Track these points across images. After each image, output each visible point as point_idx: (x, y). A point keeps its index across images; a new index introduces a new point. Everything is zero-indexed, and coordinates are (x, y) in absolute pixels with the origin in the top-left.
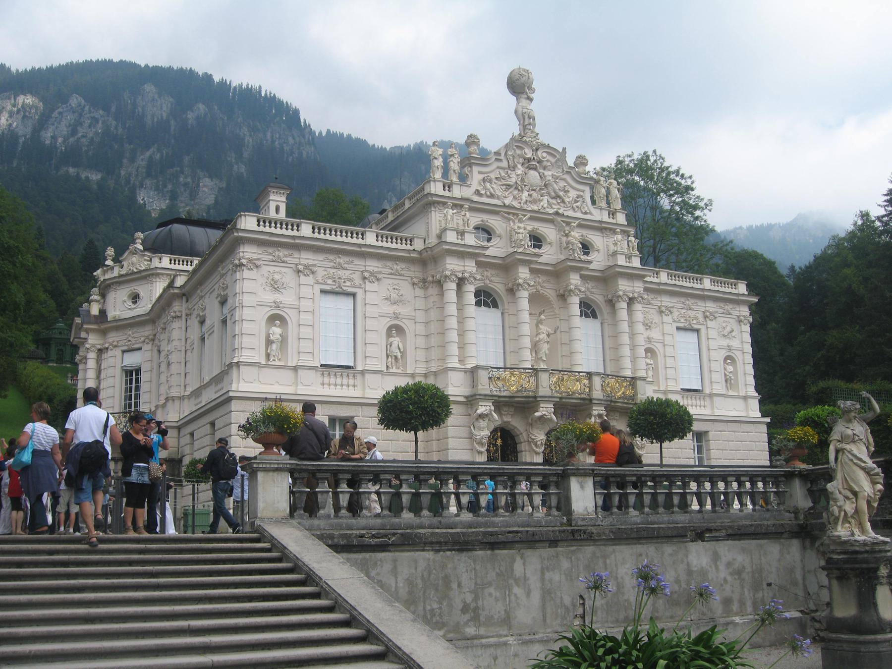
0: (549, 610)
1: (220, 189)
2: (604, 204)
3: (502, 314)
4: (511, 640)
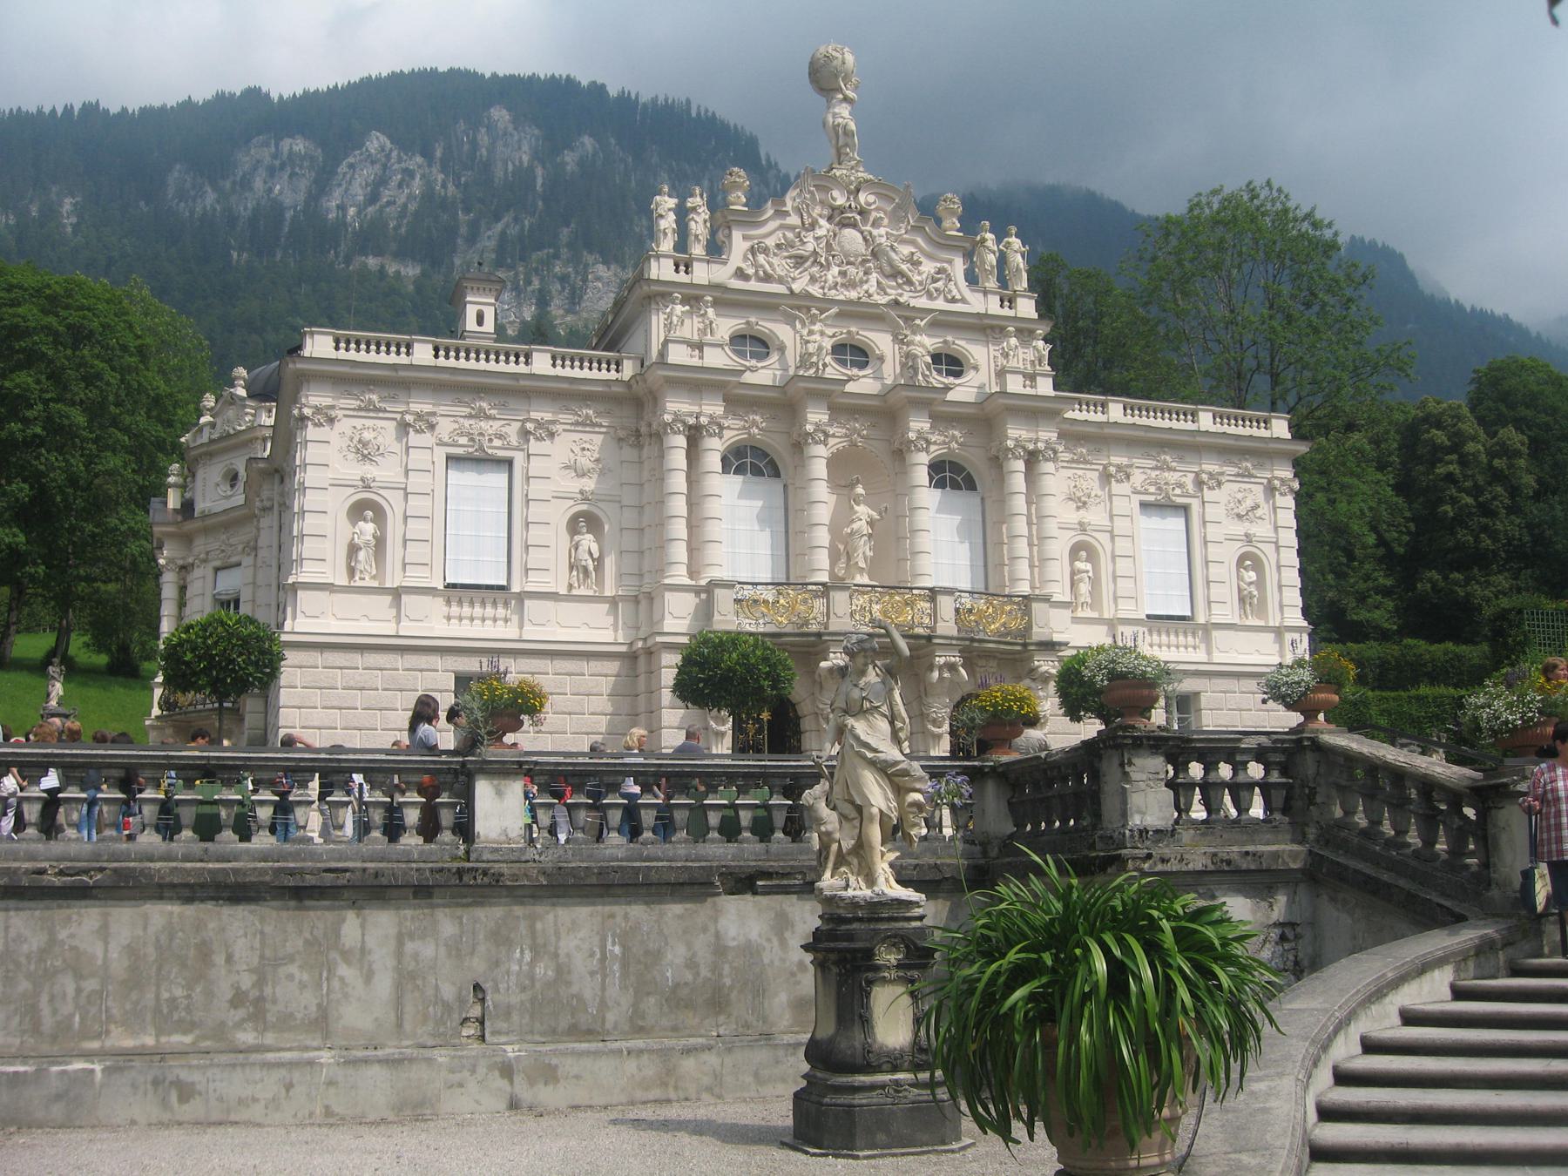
0: (409, 1009)
1: (623, 282)
2: (992, 284)
3: (785, 486)
4: (326, 1057)
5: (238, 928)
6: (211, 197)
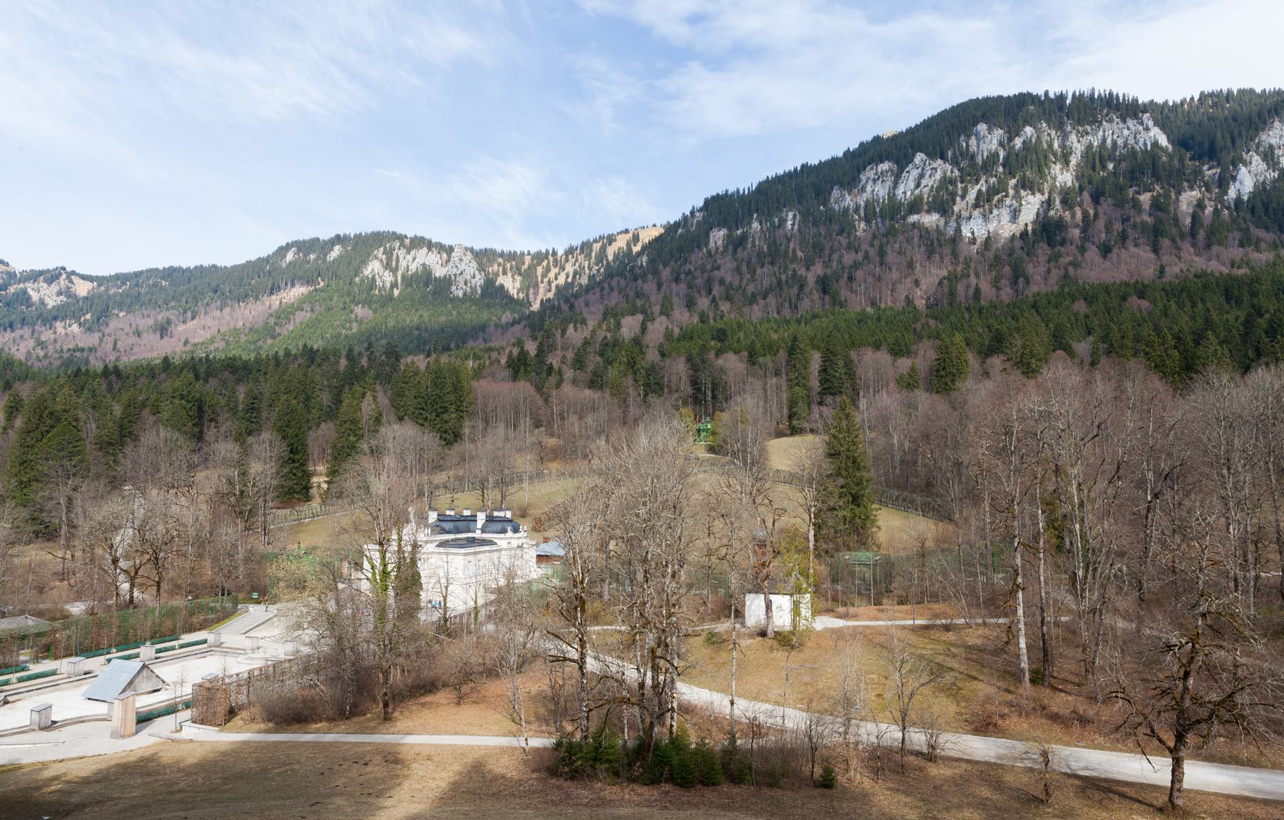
6: (848, 198)
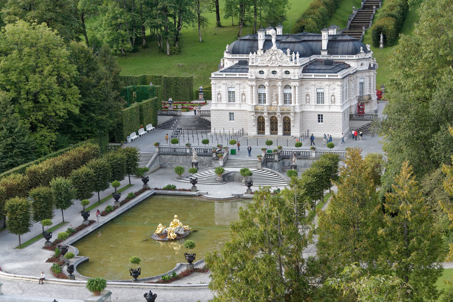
5: (174, 157)
